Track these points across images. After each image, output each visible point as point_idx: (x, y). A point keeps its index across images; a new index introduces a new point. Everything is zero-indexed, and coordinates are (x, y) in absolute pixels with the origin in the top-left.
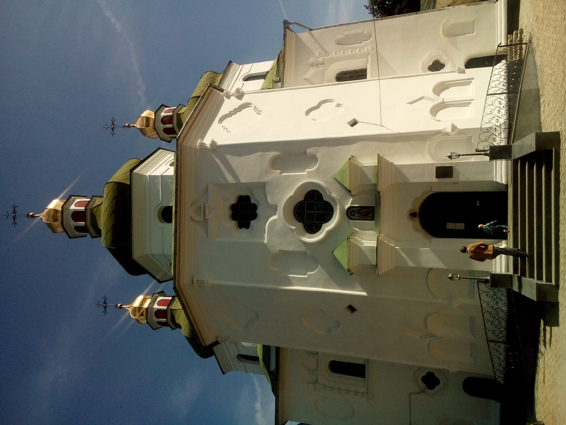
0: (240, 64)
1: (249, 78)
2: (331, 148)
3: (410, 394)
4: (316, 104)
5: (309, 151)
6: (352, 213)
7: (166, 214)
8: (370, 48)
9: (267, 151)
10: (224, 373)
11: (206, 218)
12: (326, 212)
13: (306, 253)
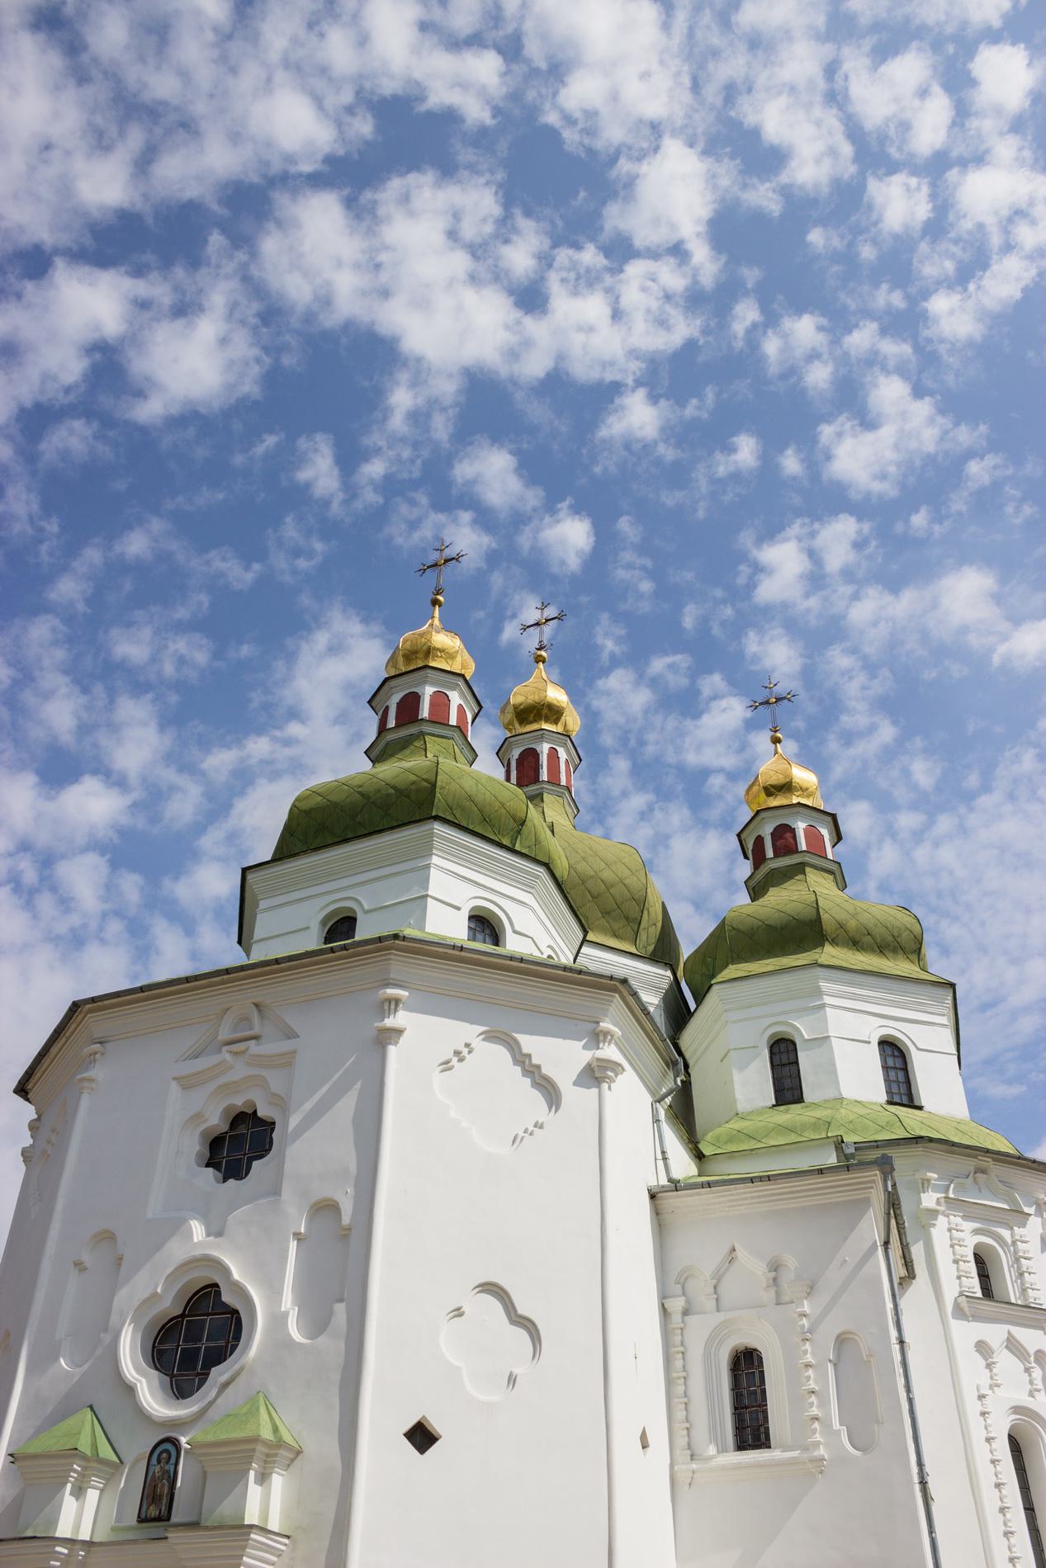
1: (893, 1052)
2: (336, 1377)
4: (520, 1311)
5: (340, 1309)
6: (166, 1450)
7: (341, 926)
8: (822, 1451)
9: (356, 1186)
11: (225, 1048)
13: (106, 1330)
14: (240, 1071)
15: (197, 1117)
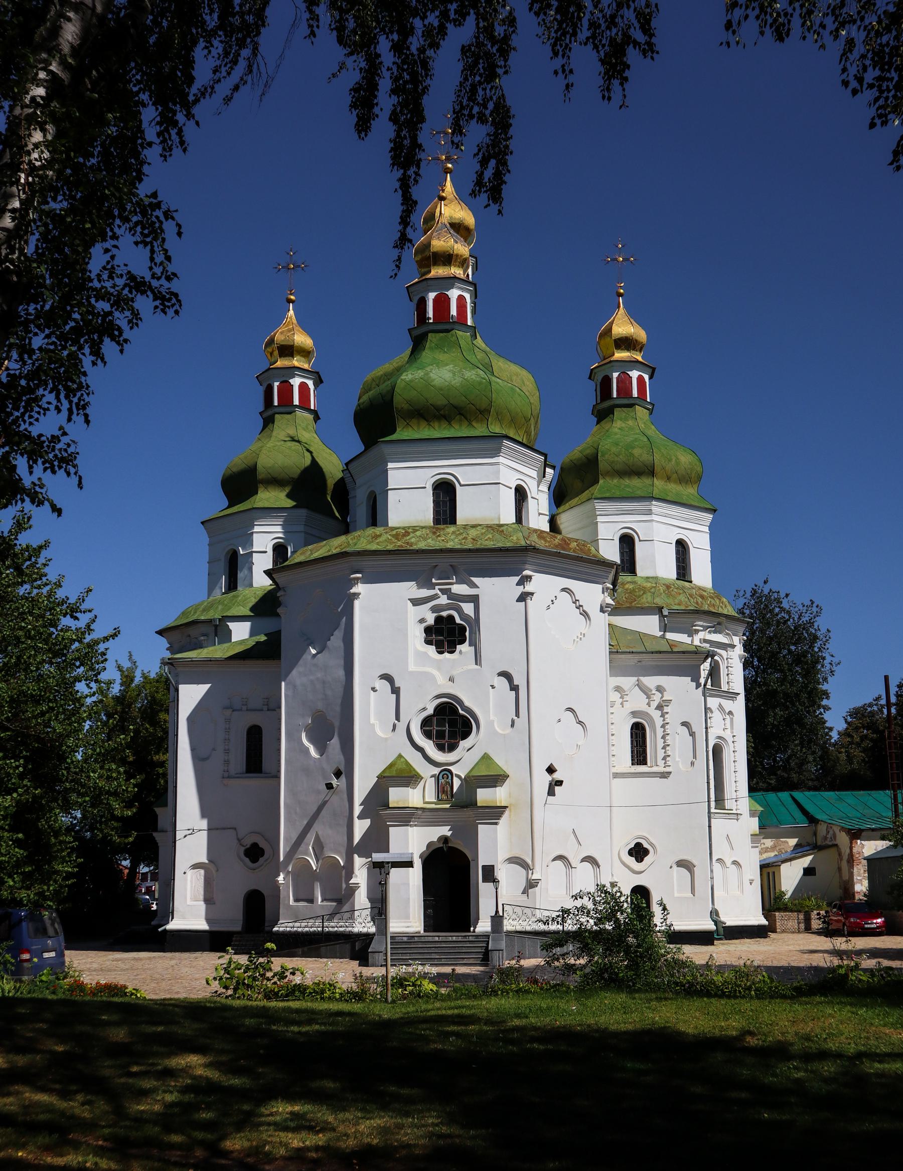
0: (710, 527)
1: (682, 548)
3: (235, 829)
10: (202, 523)
12: (447, 743)
14: (443, 600)
15: (422, 621)
